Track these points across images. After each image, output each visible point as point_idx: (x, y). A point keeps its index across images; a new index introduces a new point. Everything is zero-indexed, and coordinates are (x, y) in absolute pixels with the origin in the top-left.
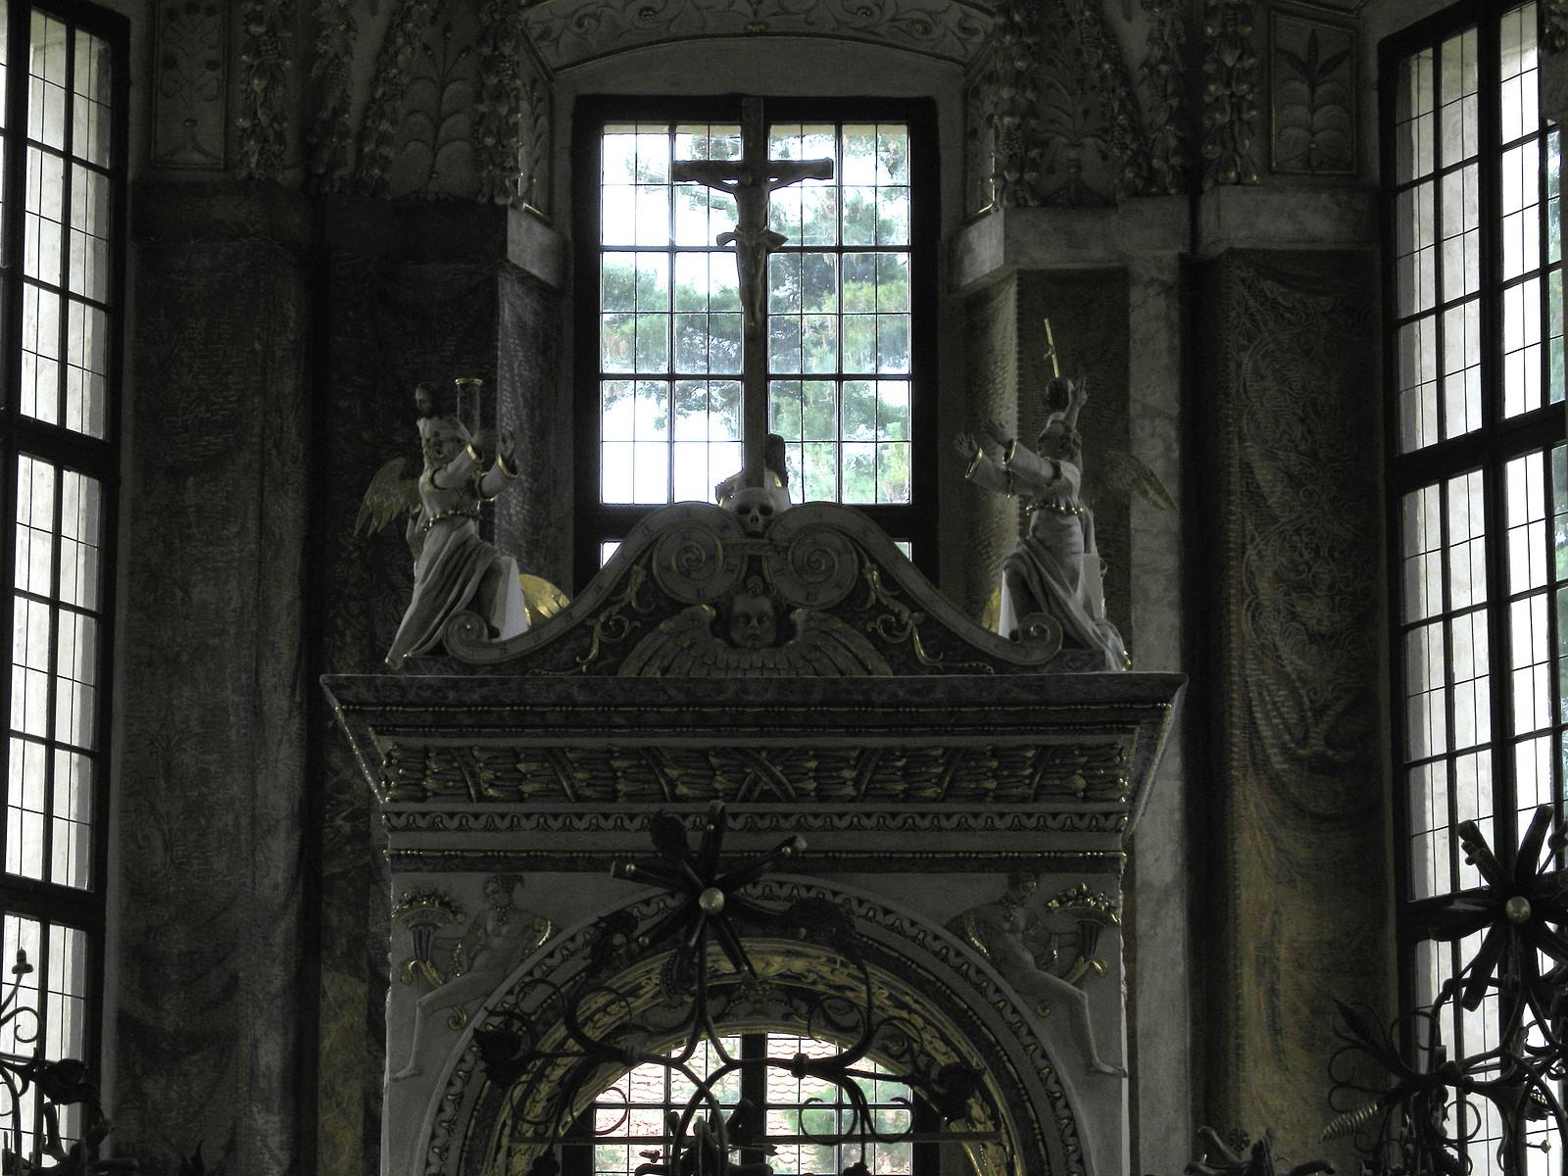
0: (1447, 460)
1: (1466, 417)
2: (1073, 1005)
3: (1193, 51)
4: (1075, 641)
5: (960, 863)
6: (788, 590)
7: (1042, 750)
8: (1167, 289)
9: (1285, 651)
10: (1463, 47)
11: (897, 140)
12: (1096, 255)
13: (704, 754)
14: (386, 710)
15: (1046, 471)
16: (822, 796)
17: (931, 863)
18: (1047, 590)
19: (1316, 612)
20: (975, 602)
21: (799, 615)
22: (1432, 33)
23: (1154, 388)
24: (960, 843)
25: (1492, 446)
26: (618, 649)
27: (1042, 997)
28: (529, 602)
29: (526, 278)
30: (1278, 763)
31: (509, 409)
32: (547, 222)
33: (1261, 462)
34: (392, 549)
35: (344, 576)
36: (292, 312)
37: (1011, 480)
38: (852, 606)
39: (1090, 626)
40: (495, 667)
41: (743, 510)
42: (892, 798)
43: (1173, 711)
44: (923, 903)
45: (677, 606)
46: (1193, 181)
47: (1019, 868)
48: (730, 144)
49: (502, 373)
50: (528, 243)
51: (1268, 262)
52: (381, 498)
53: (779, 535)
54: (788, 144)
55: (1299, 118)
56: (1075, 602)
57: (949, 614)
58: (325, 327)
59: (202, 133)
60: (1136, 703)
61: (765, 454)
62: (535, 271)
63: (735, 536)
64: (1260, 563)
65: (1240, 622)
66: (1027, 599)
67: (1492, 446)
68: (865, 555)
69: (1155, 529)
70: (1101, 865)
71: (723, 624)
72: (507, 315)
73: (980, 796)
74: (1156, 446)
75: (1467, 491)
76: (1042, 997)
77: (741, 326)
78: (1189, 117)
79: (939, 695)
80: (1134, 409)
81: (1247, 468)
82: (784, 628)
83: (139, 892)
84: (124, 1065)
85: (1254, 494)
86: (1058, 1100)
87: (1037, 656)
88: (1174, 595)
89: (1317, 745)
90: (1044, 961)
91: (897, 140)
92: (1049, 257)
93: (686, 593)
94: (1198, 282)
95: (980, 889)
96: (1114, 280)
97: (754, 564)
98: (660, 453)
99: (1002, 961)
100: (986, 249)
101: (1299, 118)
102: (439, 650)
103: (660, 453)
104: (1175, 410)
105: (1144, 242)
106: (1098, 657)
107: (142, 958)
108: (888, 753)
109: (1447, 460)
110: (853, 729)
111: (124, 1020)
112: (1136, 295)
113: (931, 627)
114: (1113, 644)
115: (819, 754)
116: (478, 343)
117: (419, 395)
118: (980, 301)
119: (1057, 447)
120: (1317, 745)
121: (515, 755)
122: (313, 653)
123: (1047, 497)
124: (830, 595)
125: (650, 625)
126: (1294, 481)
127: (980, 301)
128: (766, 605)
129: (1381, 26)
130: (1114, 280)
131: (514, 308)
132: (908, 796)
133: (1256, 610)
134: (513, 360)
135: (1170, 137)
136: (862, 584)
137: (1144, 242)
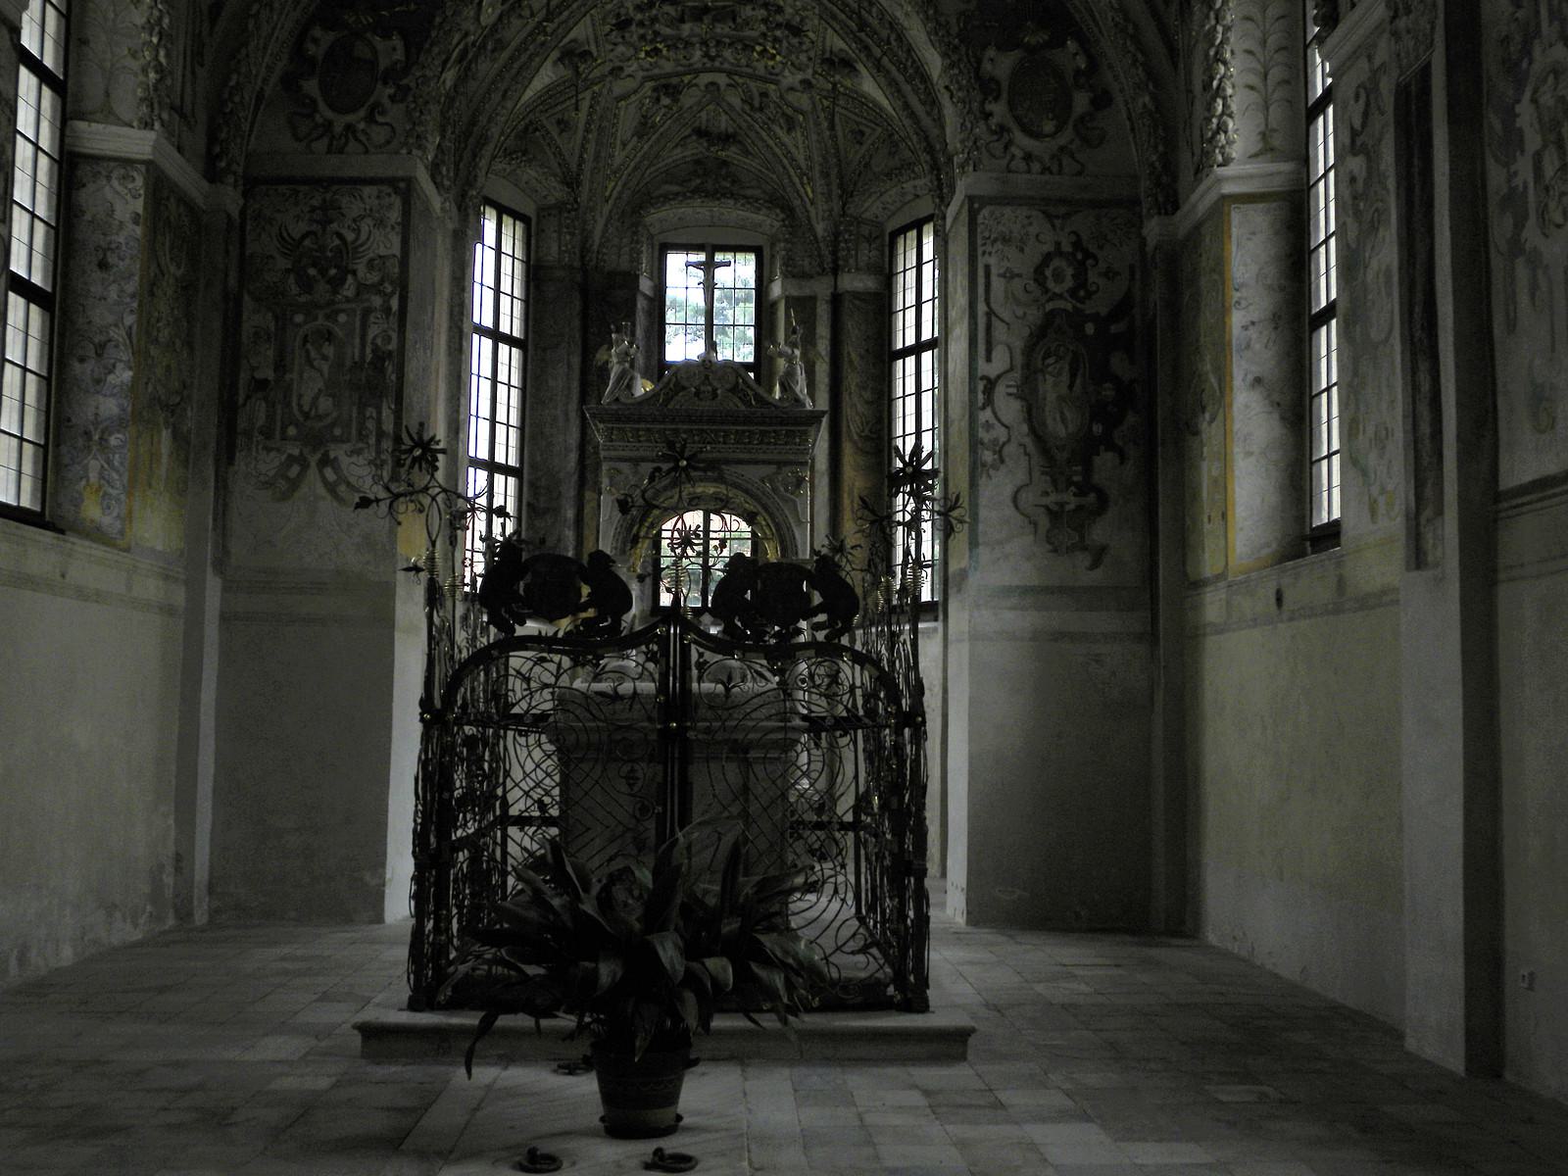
0: (906, 352)
1: (911, 341)
2: (794, 502)
3: (836, 235)
4: (797, 400)
5: (764, 462)
6: (716, 384)
7: (787, 431)
8: (827, 302)
9: (859, 406)
10: (912, 234)
11: (751, 257)
12: (807, 292)
13: (691, 430)
14: (602, 416)
15: (790, 351)
16: (725, 443)
17: (756, 462)
18: (790, 387)
19: (867, 395)
20: (771, 390)
21: (719, 392)
22: (903, 230)
23: (823, 330)
24: (761, 457)
25: (918, 349)
26: (667, 401)
27: (786, 500)
28: (643, 387)
29: (645, 295)
30: (856, 437)
31: (639, 333)
32: (651, 279)
33: (853, 351)
34: (604, 371)
35: (591, 378)
36: (578, 303)
37: (781, 354)
38: (734, 389)
39: (802, 397)
40: (633, 404)
41: (704, 361)
42: (745, 444)
43: (825, 420)
44: (753, 473)
45: (684, 388)
46: (835, 271)
47: (780, 464)
48: (702, 257)
49: (638, 323)
50: (645, 285)
51: (856, 295)
52: (601, 356)
53: (713, 368)
54: (719, 257)
55: (867, 254)
56: (797, 389)
57: (761, 391)
58: (587, 306)
59: (552, 251)
60: (814, 418)
61: (711, 345)
62: (647, 293)
63: (702, 369)
64: (852, 380)
65: (845, 396)
66: (784, 388)
67: (918, 349)
68: (738, 375)
69: (822, 370)
70: (804, 464)
71: (697, 394)
72: (639, 306)
73: (769, 443)
74: (823, 346)
75: (911, 361)
76: (786, 500)
77: (707, 306)
78: (834, 253)
79: (759, 414)
80: (817, 336)
81: (849, 353)
82: (715, 395)
83: (534, 467)
84: (529, 517)
85: (851, 362)
86: (789, 528)
87: (786, 404)
88: (828, 389)
89: (867, 432)
90: (787, 490)
91: (751, 257)
92: (795, 293)
93: (686, 384)
94: (836, 300)
95: (773, 468)
96: (813, 299)
97: (707, 377)
98: (682, 348)
99: (774, 490)
100: (776, 290)
101: (867, 254)
102: (617, 400)
103: (682, 348)
104: (829, 336)
105: (822, 288)
106: (804, 406)
107: (532, 484)
108: (744, 432)
109: (906, 352)
110: (733, 424)
111: (529, 504)
112: (818, 304)
113: (756, 395)
114: (809, 405)
115: (724, 431)
116: (631, 315)
117: (612, 327)
118: (774, 304)
119: (794, 345)
120: (867, 432)
121: (638, 430)
122: (583, 400)
123: (790, 359)
124: (728, 386)
125: (676, 394)
126: (862, 357)
127: (774, 304)
128: (710, 388)
129: (891, 226)
130: (813, 299)
131: (641, 304)
132: (749, 443)
133: (850, 393)
134: (641, 319)
135: (829, 259)
136: (737, 383)
137: (822, 288)
